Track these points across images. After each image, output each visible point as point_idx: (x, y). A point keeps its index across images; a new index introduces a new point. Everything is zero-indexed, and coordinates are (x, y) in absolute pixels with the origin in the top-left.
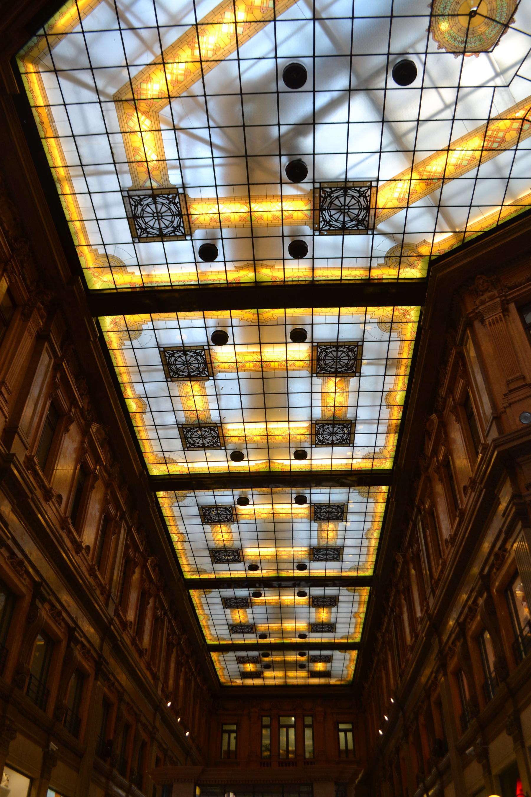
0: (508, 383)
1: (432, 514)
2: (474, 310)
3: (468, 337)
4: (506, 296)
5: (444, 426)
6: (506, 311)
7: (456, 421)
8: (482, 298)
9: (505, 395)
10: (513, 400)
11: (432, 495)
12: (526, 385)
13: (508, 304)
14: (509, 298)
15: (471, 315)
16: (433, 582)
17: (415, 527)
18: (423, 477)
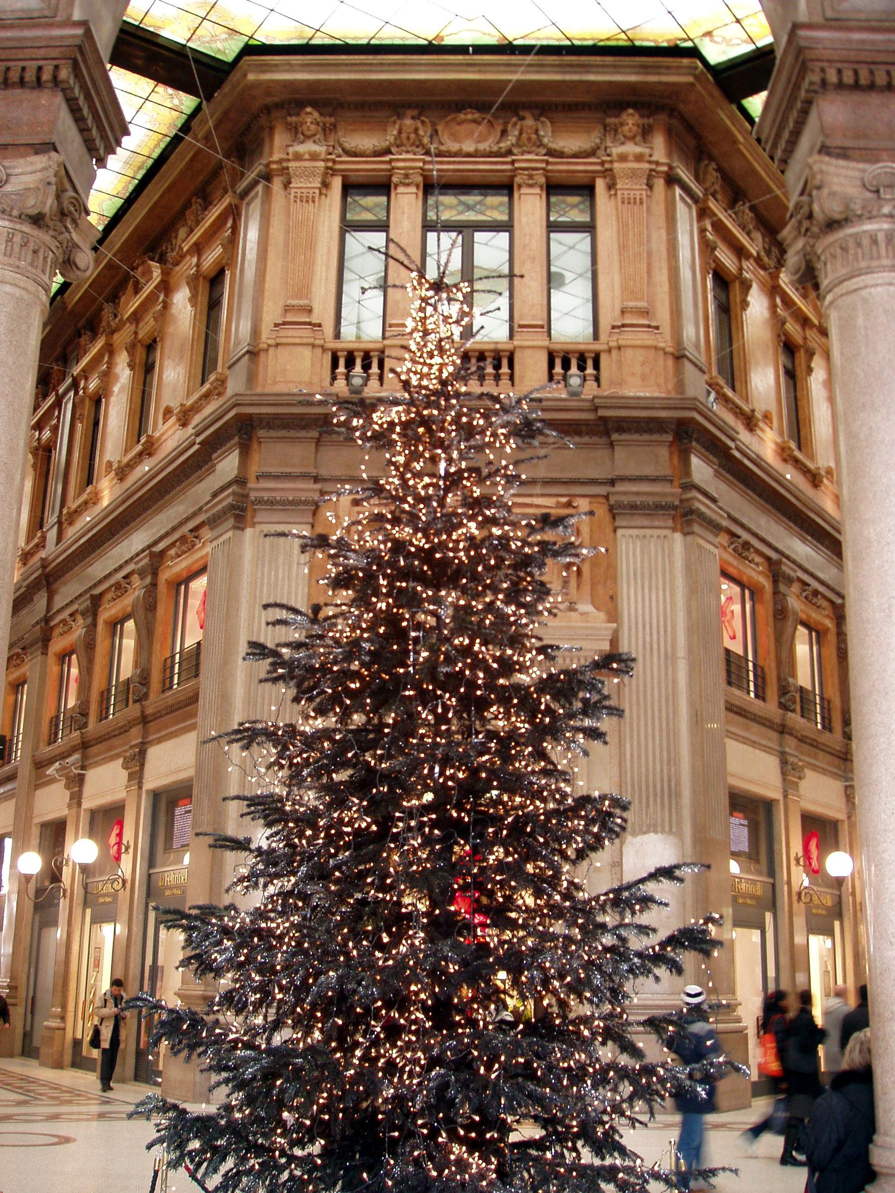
0: (287, 309)
1: (97, 401)
2: (280, 162)
3: (256, 195)
4: (334, 162)
5: (166, 287)
6: (326, 185)
7: (190, 300)
8: (301, 148)
9: (276, 325)
10: (284, 341)
11: (108, 377)
12: (309, 324)
13: (332, 175)
14: (338, 167)
15: (274, 166)
16: (65, 511)
17: (58, 404)
18: (100, 344)
